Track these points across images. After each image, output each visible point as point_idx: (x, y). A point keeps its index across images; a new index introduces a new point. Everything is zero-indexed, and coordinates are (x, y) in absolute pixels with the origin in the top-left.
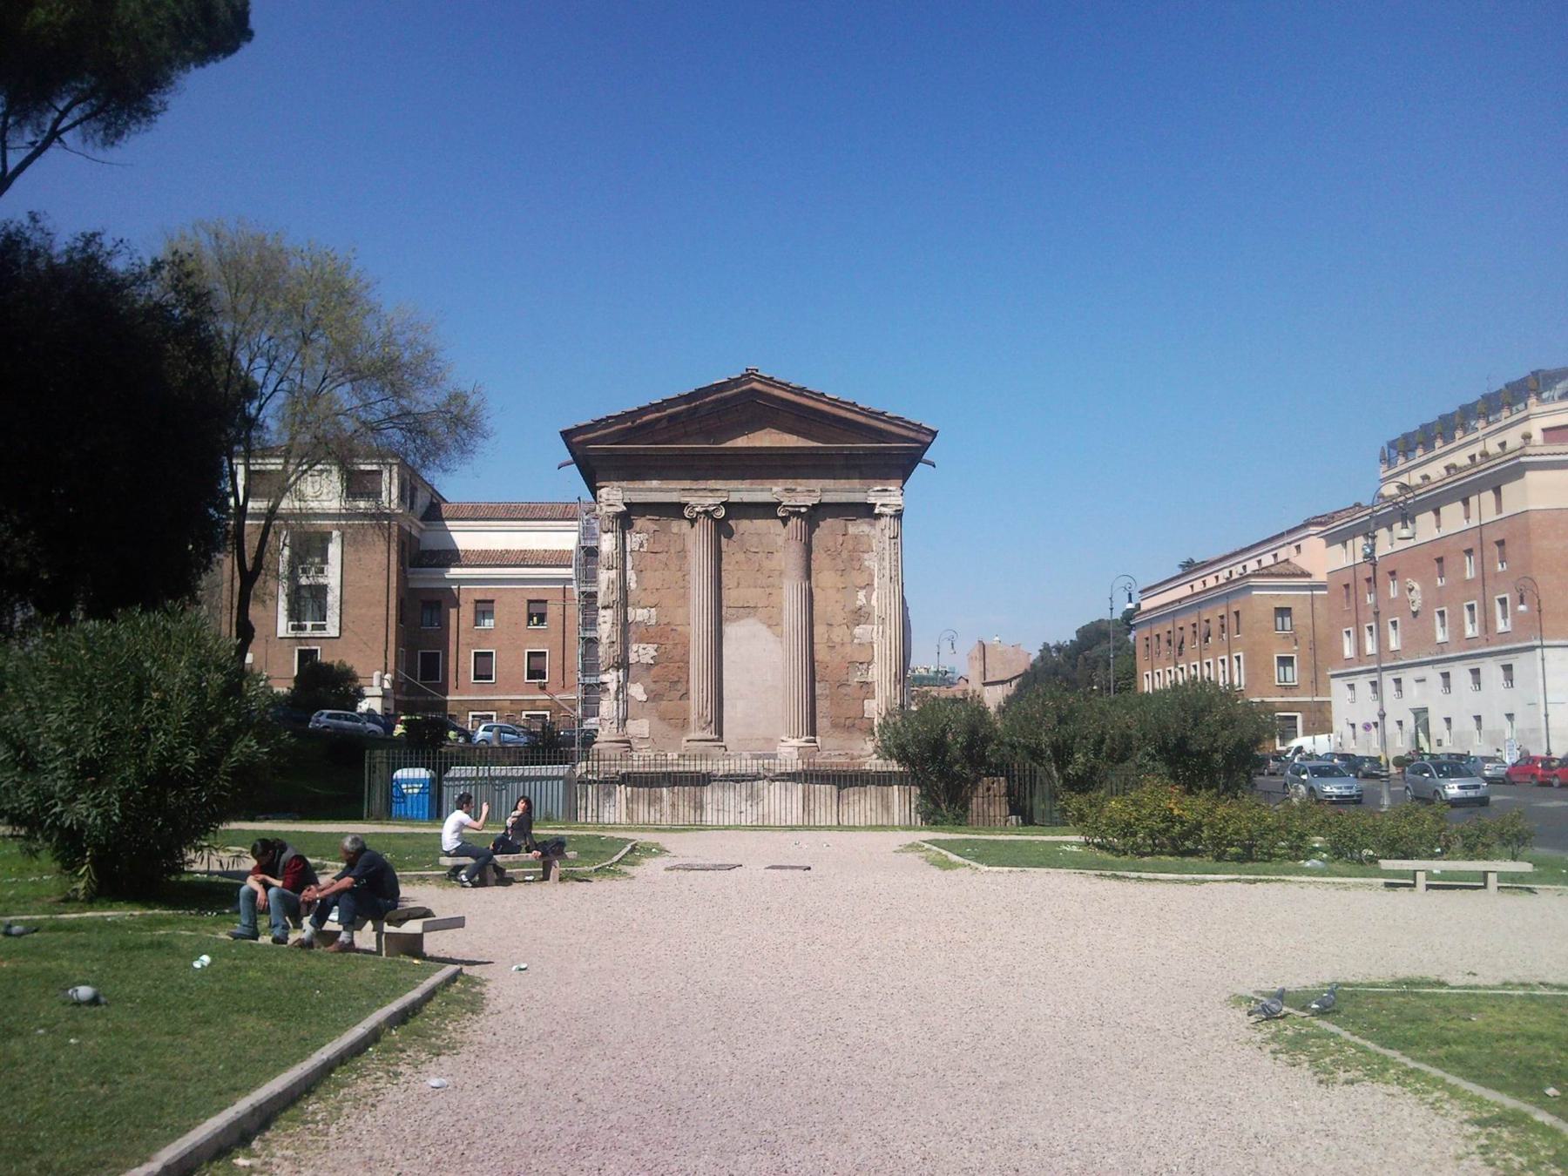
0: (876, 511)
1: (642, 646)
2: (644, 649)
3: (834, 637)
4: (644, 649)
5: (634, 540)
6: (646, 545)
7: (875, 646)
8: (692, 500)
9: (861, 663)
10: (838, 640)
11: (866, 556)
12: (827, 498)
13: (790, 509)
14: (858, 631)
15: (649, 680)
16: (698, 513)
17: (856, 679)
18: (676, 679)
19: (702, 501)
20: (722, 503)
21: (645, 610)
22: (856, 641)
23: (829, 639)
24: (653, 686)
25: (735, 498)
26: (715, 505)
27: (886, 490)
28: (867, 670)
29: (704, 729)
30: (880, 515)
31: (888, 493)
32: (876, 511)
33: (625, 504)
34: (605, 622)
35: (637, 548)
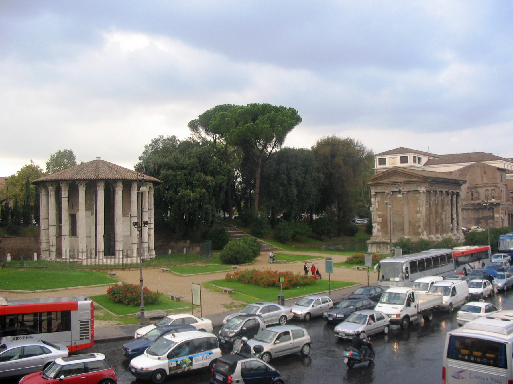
10: (414, 217)
12: (410, 190)
14: (418, 215)
17: (417, 225)
25: (394, 190)
30: (420, 193)
33: (376, 192)
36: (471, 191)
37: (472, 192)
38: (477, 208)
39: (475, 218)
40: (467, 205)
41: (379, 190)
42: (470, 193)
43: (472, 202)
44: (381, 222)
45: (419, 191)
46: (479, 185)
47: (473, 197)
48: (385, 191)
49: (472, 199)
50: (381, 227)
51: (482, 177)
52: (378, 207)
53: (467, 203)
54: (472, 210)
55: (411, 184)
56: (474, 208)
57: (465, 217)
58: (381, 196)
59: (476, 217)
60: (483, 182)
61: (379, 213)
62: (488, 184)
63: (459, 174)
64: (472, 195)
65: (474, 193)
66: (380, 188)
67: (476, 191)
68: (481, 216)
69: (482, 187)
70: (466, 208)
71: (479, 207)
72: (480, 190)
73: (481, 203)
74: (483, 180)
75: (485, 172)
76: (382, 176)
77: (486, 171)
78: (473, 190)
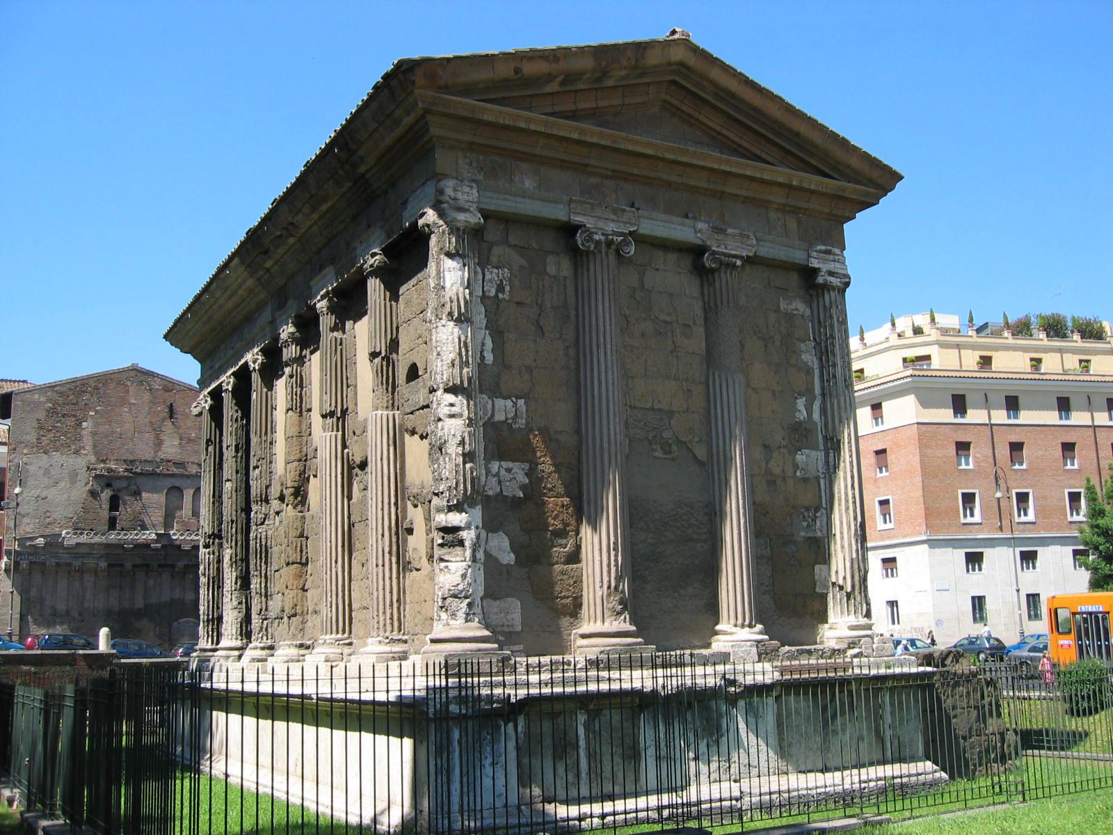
0: (820, 280)
1: (505, 464)
2: (509, 470)
3: (772, 464)
4: (509, 470)
5: (488, 276)
6: (507, 288)
7: (822, 482)
8: (590, 222)
9: (808, 509)
10: (777, 471)
11: (803, 346)
14: (800, 458)
16: (598, 243)
19: (601, 224)
20: (631, 233)
21: (509, 403)
22: (798, 474)
23: (769, 472)
26: (621, 234)
27: (828, 252)
28: (814, 520)
29: (619, 614)
30: (826, 287)
31: (831, 257)
32: (820, 280)
33: (481, 211)
35: (493, 292)
41: (524, 194)
43: (113, 537)
44: (515, 503)
45: (815, 272)
48: (578, 219)
50: (514, 548)
52: (489, 357)
55: (763, 204)
57: (61, 607)
58: (518, 260)
66: (528, 183)
68: (139, 603)
74: (159, 443)
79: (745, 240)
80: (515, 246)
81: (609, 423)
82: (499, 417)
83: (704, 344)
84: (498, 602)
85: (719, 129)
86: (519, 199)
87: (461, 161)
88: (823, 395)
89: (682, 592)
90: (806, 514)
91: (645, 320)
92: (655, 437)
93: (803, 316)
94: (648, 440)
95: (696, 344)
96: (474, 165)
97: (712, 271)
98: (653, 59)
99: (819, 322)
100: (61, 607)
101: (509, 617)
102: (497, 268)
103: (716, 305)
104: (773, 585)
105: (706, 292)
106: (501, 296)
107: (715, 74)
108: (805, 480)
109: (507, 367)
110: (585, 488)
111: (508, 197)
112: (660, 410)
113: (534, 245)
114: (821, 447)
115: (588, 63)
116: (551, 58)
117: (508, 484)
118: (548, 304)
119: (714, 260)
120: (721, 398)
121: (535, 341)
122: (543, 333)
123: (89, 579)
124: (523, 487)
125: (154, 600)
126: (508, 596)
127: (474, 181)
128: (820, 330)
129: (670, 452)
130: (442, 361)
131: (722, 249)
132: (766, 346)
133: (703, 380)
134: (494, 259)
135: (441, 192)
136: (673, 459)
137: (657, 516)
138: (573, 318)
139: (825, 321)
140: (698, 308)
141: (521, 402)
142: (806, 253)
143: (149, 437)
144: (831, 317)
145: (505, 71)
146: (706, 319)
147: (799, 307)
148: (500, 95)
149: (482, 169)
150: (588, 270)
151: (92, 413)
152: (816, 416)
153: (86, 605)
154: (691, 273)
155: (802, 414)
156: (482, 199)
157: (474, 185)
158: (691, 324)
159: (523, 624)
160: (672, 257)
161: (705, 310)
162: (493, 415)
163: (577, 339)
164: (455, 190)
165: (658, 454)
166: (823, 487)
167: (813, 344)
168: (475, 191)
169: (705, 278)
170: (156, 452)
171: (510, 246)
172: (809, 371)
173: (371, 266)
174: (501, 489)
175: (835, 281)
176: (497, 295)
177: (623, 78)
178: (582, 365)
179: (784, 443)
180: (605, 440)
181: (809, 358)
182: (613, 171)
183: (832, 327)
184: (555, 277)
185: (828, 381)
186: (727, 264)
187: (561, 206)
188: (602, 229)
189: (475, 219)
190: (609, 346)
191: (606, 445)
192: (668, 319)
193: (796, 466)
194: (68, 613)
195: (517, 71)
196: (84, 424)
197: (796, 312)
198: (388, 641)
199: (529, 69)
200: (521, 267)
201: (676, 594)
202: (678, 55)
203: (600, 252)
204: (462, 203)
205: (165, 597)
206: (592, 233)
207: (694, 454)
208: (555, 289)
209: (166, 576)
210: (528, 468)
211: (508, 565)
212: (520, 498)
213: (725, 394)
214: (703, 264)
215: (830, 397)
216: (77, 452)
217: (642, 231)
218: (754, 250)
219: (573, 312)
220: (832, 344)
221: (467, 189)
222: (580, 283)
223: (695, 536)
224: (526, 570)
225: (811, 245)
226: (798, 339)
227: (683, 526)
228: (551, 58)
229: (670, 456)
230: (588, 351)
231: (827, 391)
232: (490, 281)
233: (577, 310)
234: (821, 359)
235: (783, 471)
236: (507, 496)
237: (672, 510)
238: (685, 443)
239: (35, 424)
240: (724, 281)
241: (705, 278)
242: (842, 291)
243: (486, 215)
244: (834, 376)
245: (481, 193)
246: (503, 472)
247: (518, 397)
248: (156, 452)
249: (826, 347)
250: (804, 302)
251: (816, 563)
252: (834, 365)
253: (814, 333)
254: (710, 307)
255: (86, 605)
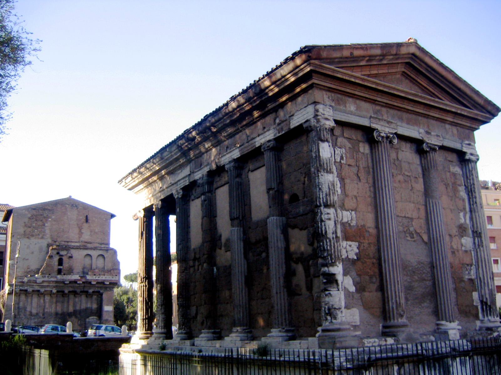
0: (467, 157)
4: (350, 246)
6: (345, 158)
7: (473, 252)
9: (468, 265)
10: (455, 247)
13: (431, 146)
15: (354, 273)
16: (383, 137)
18: (372, 273)
21: (348, 213)
22: (463, 248)
24: (358, 279)
26: (392, 133)
27: (469, 144)
28: (471, 270)
30: (469, 161)
31: (471, 147)
32: (467, 157)
33: (336, 121)
34: (329, 219)
35: (338, 160)
36: (58, 253)
37: (62, 256)
38: (66, 291)
39: (57, 314)
40: (45, 284)
41: (351, 113)
42: (56, 258)
44: (354, 262)
45: (465, 153)
46: (73, 244)
47: (61, 267)
48: (374, 126)
49: (60, 272)
51: (80, 228)
53: (46, 279)
54: (51, 294)
56: (61, 293)
57: (34, 311)
59: (59, 310)
60: (82, 239)
61: (346, 216)
62: (91, 243)
63: (29, 215)
64: (60, 262)
65: (65, 258)
66: (353, 108)
67: (69, 255)
68: (71, 309)
69: (78, 248)
70: (42, 290)
71: (71, 289)
72: (74, 252)
73: (79, 280)
74: (81, 233)
75: (87, 220)
76: (376, 56)
77: (89, 218)
78: (62, 253)
79: (438, 138)
80: (347, 138)
81: (392, 223)
82: (345, 220)
83: (423, 187)
84: (349, 310)
85: (425, 85)
86: (349, 115)
87: (325, 96)
88: (471, 211)
89: (423, 305)
90: (467, 268)
91: (400, 174)
92: (407, 230)
93: (459, 174)
94: (404, 231)
95: (420, 186)
96: (330, 98)
97: (426, 152)
98: (404, 50)
99: (467, 177)
100: (34, 311)
101: (355, 318)
102: (340, 148)
103: (428, 168)
104: (457, 301)
105: (423, 162)
106: (342, 161)
107: (427, 60)
108: (466, 251)
109: (347, 196)
110: (382, 254)
111: (345, 114)
112: (408, 217)
113: (354, 138)
114: (471, 236)
115: (378, 52)
116: (365, 49)
117: (350, 252)
118: (361, 166)
119: (428, 147)
120: (434, 212)
121: (357, 184)
122: (360, 180)
123: (47, 298)
124: (356, 254)
125: (78, 308)
126: (353, 307)
127: (331, 106)
128: (467, 181)
129: (413, 238)
130: (322, 192)
131: (429, 142)
132: (447, 188)
133: (424, 203)
134: (338, 144)
135: (317, 111)
136: (414, 241)
137: (411, 268)
138: (371, 173)
139: (470, 176)
140: (420, 170)
141: (353, 213)
142: (461, 145)
143: (76, 230)
144: (472, 175)
145: (346, 53)
146: (424, 175)
147: (457, 170)
148: (340, 66)
149: (333, 101)
150: (378, 150)
151: (50, 220)
152: (468, 221)
153: (46, 310)
154: (416, 153)
155: (462, 221)
156: (335, 115)
157: (331, 108)
158: (417, 177)
159: (360, 321)
160: (408, 145)
161: (423, 171)
162: (342, 219)
163: (374, 183)
164: (324, 110)
165: (409, 238)
166: (473, 255)
167: (464, 187)
168: (331, 111)
169: (422, 156)
170: (80, 238)
171: (345, 138)
172: (463, 200)
173: (268, 147)
174: (348, 256)
175: (473, 158)
176: (340, 162)
177: (390, 60)
178: (377, 195)
179: (457, 234)
180: (391, 232)
181: (463, 194)
182: (386, 103)
183: (473, 179)
184: (363, 153)
185: (473, 205)
186: (433, 149)
187: (367, 119)
188: (384, 131)
189: (332, 124)
190: (390, 187)
191: (392, 234)
192: (409, 174)
193: (462, 245)
194: (37, 314)
195: (352, 53)
196: (46, 225)
197: (456, 172)
198: (284, 330)
199: (357, 53)
200: (349, 148)
201: (420, 306)
202: (413, 50)
203: (383, 142)
204: (326, 116)
205: (83, 306)
206: (380, 132)
207: (423, 239)
208: (364, 159)
209: (83, 297)
210: (358, 245)
211: (353, 292)
212: (355, 259)
213: (435, 210)
214: (423, 149)
215: (475, 211)
216: (42, 238)
217: (399, 133)
218: (442, 142)
219: (371, 170)
220: (474, 188)
221: (328, 110)
222: (374, 156)
223: (426, 278)
224: (359, 295)
225: (463, 141)
226: (458, 185)
227: (421, 273)
228: (365, 49)
229: (413, 240)
230: (380, 189)
231: (472, 210)
232: (338, 154)
233: (373, 169)
234: (468, 195)
235: (457, 247)
236: (350, 259)
237: (416, 265)
238: (419, 233)
239: (23, 225)
240: (431, 156)
241: (422, 156)
242: (476, 162)
243: (336, 121)
244: (476, 203)
245: (334, 112)
246: (348, 247)
247: (352, 210)
248: (80, 238)
249: (471, 189)
250: (460, 168)
251: (473, 291)
252: (475, 198)
253: (464, 182)
254: (426, 169)
255: (46, 310)
